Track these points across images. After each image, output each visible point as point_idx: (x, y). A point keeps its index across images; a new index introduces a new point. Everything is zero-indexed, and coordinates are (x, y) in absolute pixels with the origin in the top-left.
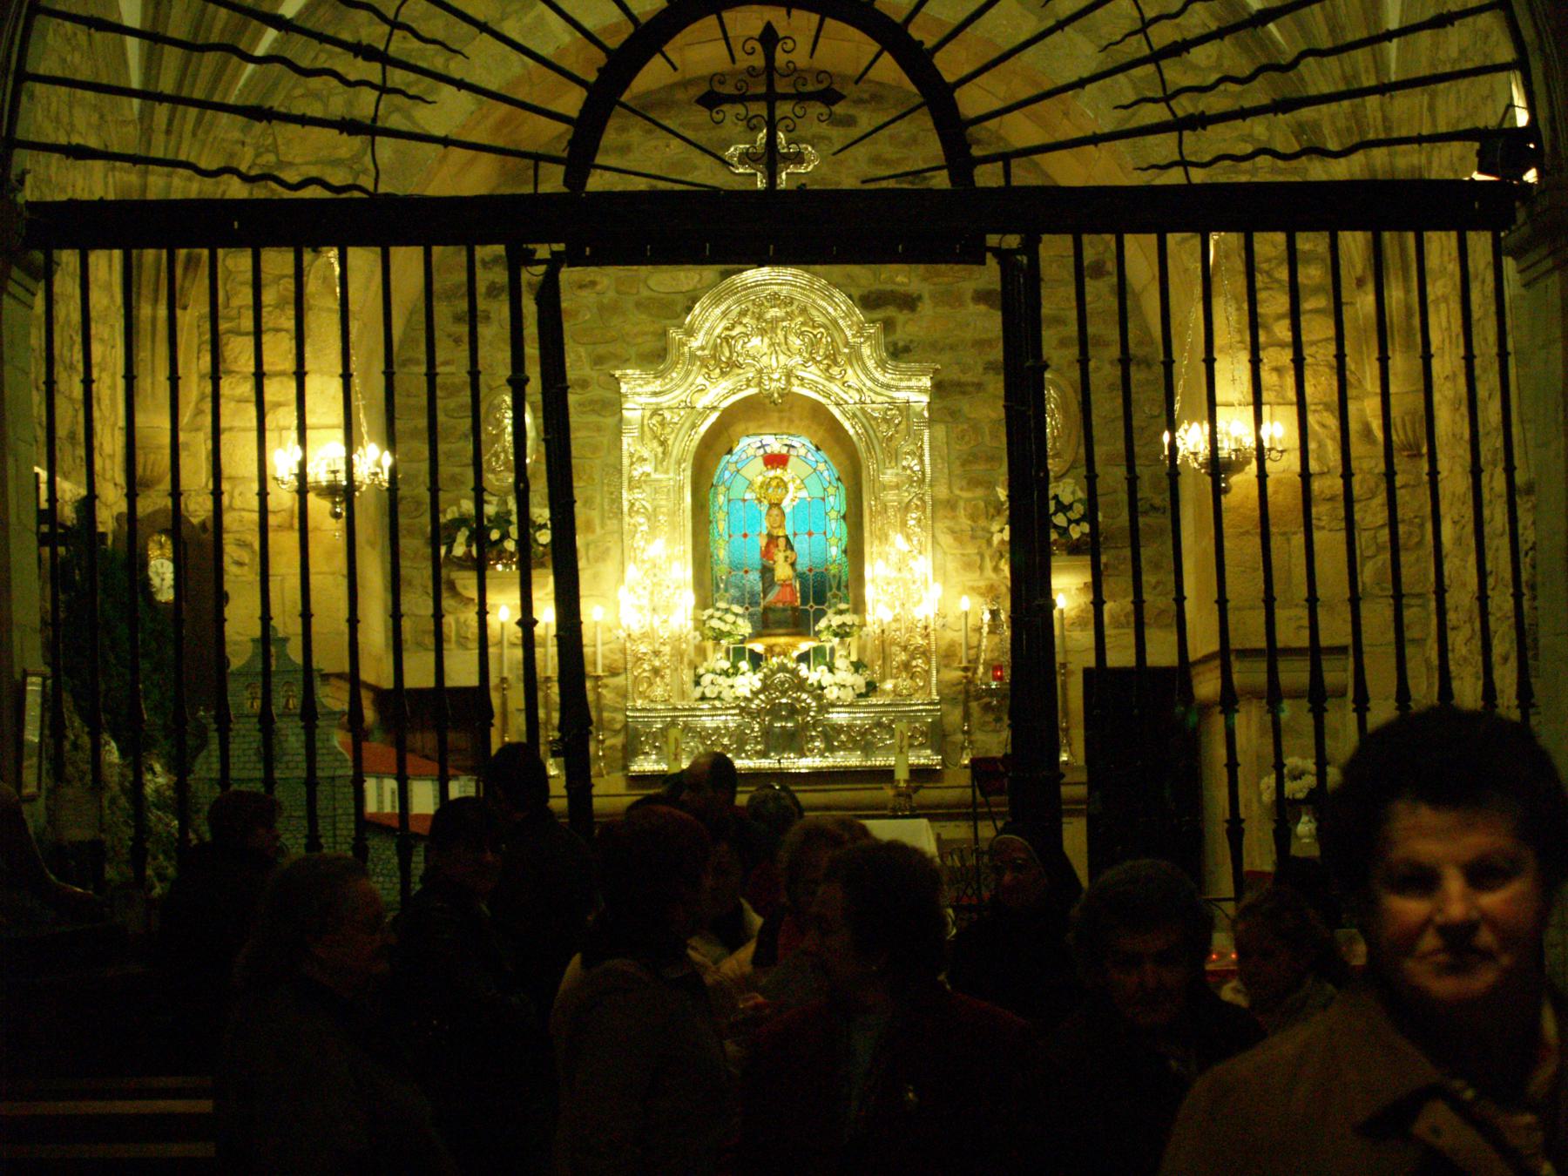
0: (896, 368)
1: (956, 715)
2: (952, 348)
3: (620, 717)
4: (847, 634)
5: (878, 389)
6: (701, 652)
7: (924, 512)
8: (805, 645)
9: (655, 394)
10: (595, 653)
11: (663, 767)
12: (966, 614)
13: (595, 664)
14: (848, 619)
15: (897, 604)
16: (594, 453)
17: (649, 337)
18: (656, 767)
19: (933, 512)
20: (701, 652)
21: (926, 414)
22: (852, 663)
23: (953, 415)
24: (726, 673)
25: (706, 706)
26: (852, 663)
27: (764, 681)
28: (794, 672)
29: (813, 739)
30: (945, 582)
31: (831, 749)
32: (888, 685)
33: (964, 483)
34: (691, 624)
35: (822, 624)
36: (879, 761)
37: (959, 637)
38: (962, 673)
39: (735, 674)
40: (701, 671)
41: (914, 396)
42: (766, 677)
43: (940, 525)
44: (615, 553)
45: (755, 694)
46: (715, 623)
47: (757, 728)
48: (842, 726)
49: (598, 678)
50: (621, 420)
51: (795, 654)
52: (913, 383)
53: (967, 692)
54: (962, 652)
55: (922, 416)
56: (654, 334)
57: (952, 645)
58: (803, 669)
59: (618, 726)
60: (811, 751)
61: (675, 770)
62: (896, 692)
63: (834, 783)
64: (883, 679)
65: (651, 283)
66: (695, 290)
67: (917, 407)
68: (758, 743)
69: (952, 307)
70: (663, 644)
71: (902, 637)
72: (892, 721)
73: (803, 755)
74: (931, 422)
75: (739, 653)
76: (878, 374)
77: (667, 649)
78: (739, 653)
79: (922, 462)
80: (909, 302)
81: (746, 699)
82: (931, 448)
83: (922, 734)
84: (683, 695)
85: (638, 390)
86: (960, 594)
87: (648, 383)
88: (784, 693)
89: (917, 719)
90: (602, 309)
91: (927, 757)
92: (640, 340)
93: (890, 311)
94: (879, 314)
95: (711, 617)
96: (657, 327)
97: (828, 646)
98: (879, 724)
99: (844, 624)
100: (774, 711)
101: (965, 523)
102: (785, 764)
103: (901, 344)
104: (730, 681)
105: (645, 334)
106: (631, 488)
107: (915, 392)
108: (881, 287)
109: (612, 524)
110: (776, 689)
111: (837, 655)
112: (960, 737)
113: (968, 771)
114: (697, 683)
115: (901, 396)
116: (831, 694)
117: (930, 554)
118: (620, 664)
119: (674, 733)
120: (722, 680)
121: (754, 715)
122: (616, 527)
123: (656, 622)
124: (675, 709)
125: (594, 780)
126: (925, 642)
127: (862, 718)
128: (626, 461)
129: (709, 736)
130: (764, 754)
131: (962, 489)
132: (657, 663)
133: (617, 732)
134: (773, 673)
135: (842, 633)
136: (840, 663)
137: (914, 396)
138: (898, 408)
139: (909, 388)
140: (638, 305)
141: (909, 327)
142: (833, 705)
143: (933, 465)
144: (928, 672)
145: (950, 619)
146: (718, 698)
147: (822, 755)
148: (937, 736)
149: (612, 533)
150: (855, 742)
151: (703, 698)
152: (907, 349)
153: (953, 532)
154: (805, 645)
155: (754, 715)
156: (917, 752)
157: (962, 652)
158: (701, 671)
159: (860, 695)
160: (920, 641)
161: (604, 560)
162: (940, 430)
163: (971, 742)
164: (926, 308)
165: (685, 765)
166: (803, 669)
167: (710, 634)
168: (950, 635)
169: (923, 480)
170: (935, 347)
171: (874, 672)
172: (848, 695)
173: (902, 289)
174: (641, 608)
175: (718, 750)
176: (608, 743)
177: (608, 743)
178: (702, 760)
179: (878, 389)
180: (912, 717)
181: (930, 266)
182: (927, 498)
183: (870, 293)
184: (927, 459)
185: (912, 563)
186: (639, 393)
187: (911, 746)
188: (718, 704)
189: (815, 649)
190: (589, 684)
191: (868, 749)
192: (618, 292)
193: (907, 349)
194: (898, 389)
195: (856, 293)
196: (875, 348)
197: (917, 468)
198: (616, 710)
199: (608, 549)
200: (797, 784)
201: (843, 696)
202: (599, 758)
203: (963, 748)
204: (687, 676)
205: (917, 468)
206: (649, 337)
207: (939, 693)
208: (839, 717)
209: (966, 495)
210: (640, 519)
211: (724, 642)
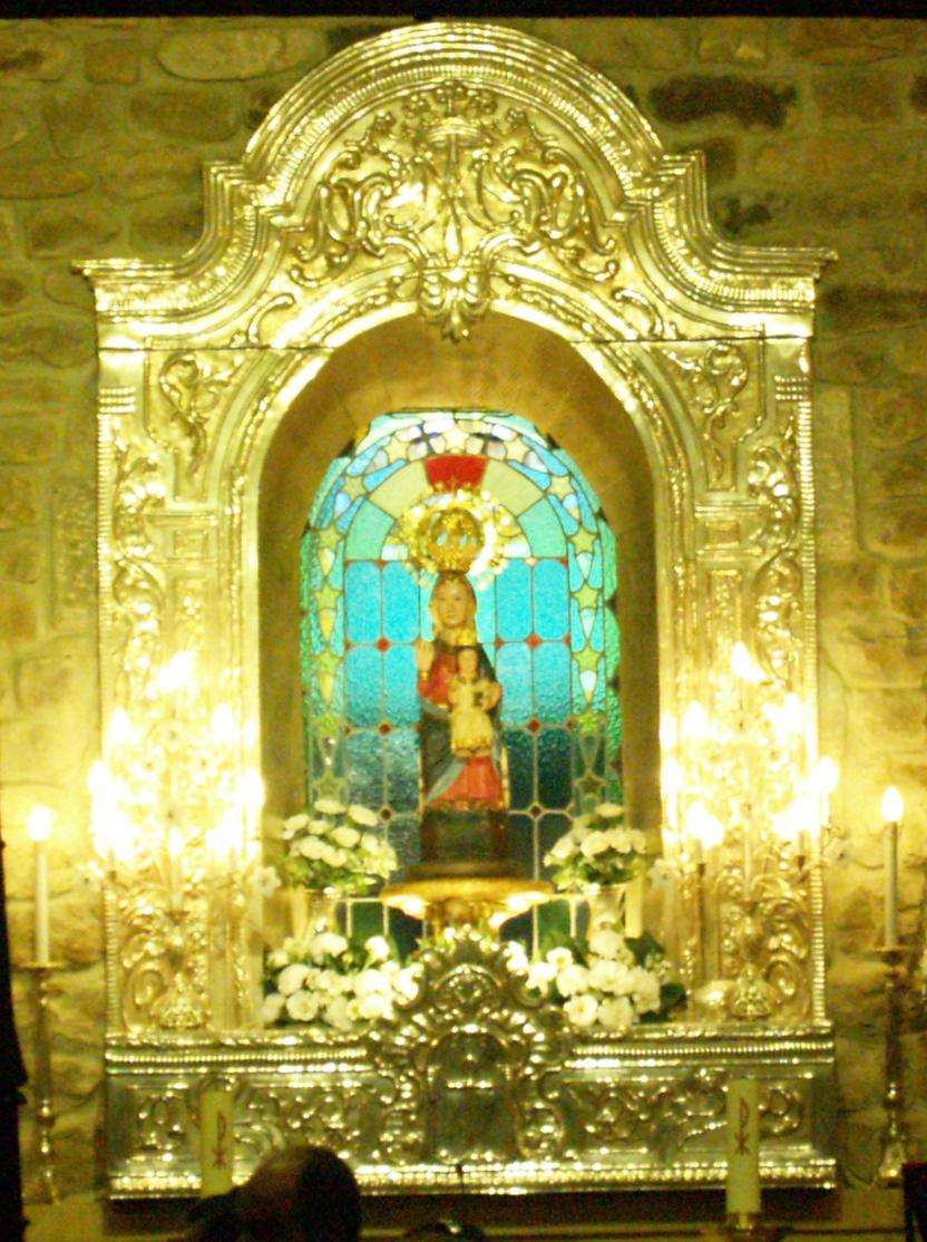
0: (734, 259)
1: (868, 1065)
2: (865, 211)
3: (89, 1064)
4: (620, 876)
5: (694, 307)
6: (280, 914)
7: (798, 592)
8: (521, 900)
9: (176, 315)
10: (33, 916)
11: (191, 1181)
12: (895, 831)
13: (33, 940)
14: (621, 839)
15: (735, 805)
16: (32, 451)
17: (162, 184)
18: (174, 1182)
19: (819, 592)
20: (280, 914)
21: (804, 366)
22: (629, 942)
23: (868, 367)
24: (336, 964)
25: (289, 1039)
26: (629, 942)
27: (424, 982)
28: (495, 963)
29: (537, 1117)
30: (846, 756)
31: (580, 1141)
32: (713, 994)
33: (891, 526)
34: (256, 850)
35: (561, 851)
36: (689, 1170)
37: (878, 882)
38: (882, 967)
39: (358, 966)
40: (279, 958)
41: (775, 324)
42: (429, 972)
43: (836, 624)
44: (81, 683)
45: (405, 1012)
46: (312, 848)
47: (407, 1090)
48: (604, 1088)
49: (39, 974)
50: (96, 374)
51: (497, 920)
52: (775, 292)
53: (896, 1010)
54: (885, 919)
55: (796, 370)
56: (175, 175)
57: (862, 901)
58: (515, 956)
59: (85, 1086)
60: (533, 1144)
61: (218, 1188)
62: (729, 1008)
63: (585, 1219)
64: (702, 979)
65: (169, 57)
66: (270, 72)
67: (784, 349)
68: (410, 1126)
69: (866, 116)
70: (191, 895)
71: (744, 881)
72: (722, 1078)
73: (514, 1155)
74: (816, 384)
75: (366, 918)
76: (693, 272)
77: (199, 908)
78: (366, 918)
79: (793, 475)
80: (765, 106)
81: (382, 1024)
82: (816, 444)
83: (791, 1106)
84: (237, 1014)
85: (137, 305)
86: (881, 783)
87: (159, 289)
88: (471, 1011)
89: (778, 1073)
90: (53, 117)
91: (802, 1162)
92: (140, 190)
93: (722, 127)
94: (697, 132)
95: (303, 833)
96: (182, 160)
97: (573, 901)
98: (691, 1085)
99: (611, 852)
100: (448, 1052)
101: (893, 618)
102: (473, 1175)
103: (746, 202)
104: (346, 983)
105: (155, 175)
106: (118, 534)
107: (779, 314)
108: (703, 70)
109: (74, 617)
110: (454, 1002)
111: (595, 922)
112: (878, 1115)
113: (898, 1194)
114: (270, 987)
115: (747, 323)
116: (581, 1013)
117: (810, 691)
118: (92, 941)
119: (215, 1103)
120: (326, 979)
121: (402, 1061)
122: (82, 624)
123: (176, 842)
124: (219, 1047)
125: (29, 1211)
126: (798, 895)
127: (651, 1069)
128: (107, 471)
129: (297, 1110)
130: (424, 1153)
131: (885, 539)
132: (177, 940)
133: (82, 1100)
134: (447, 963)
135: (606, 871)
136: (602, 941)
137: (775, 324)
138: (740, 352)
139: (766, 304)
140: (138, 108)
141: (766, 164)
142: (584, 1039)
143: (820, 482)
144: (805, 964)
145: (858, 842)
146: (319, 1021)
147: (558, 1155)
148: (824, 1112)
149: (73, 636)
150: (635, 1125)
151: (283, 1021)
152: (760, 215)
153: (863, 638)
154: (521, 900)
155: (402, 1061)
156: (779, 1149)
157: (885, 919)
158: (279, 958)
159: (647, 1017)
160: (787, 892)
161: (55, 700)
162: (837, 403)
163: (903, 1127)
164: (805, 118)
165: (241, 1176)
166: (515, 956)
167: (301, 872)
168: (856, 878)
169: (794, 520)
170: (826, 210)
171: (679, 964)
172: (620, 1017)
173: (749, 75)
174: (140, 812)
175: (318, 1141)
176: (63, 1124)
177: (63, 1124)
178: (280, 1166)
179: (694, 307)
180: (767, 1069)
181: (813, 22)
182: (806, 560)
183: (675, 82)
184: (805, 469)
185: (769, 711)
186: (140, 313)
187: (765, 1135)
188: (317, 1034)
189: (545, 910)
190: (18, 988)
191: (664, 1141)
192: (90, 78)
193: (760, 215)
194: (739, 306)
195: (644, 84)
196: (686, 211)
197: (781, 490)
198: (80, 1048)
199: (63, 677)
200: (500, 1221)
201: (607, 1020)
202: (42, 1158)
203: (885, 1141)
204: (247, 970)
205: (781, 490)
206: (162, 184)
207: (830, 1013)
208: (599, 1067)
209: (894, 553)
210: (141, 606)
211: (333, 892)
